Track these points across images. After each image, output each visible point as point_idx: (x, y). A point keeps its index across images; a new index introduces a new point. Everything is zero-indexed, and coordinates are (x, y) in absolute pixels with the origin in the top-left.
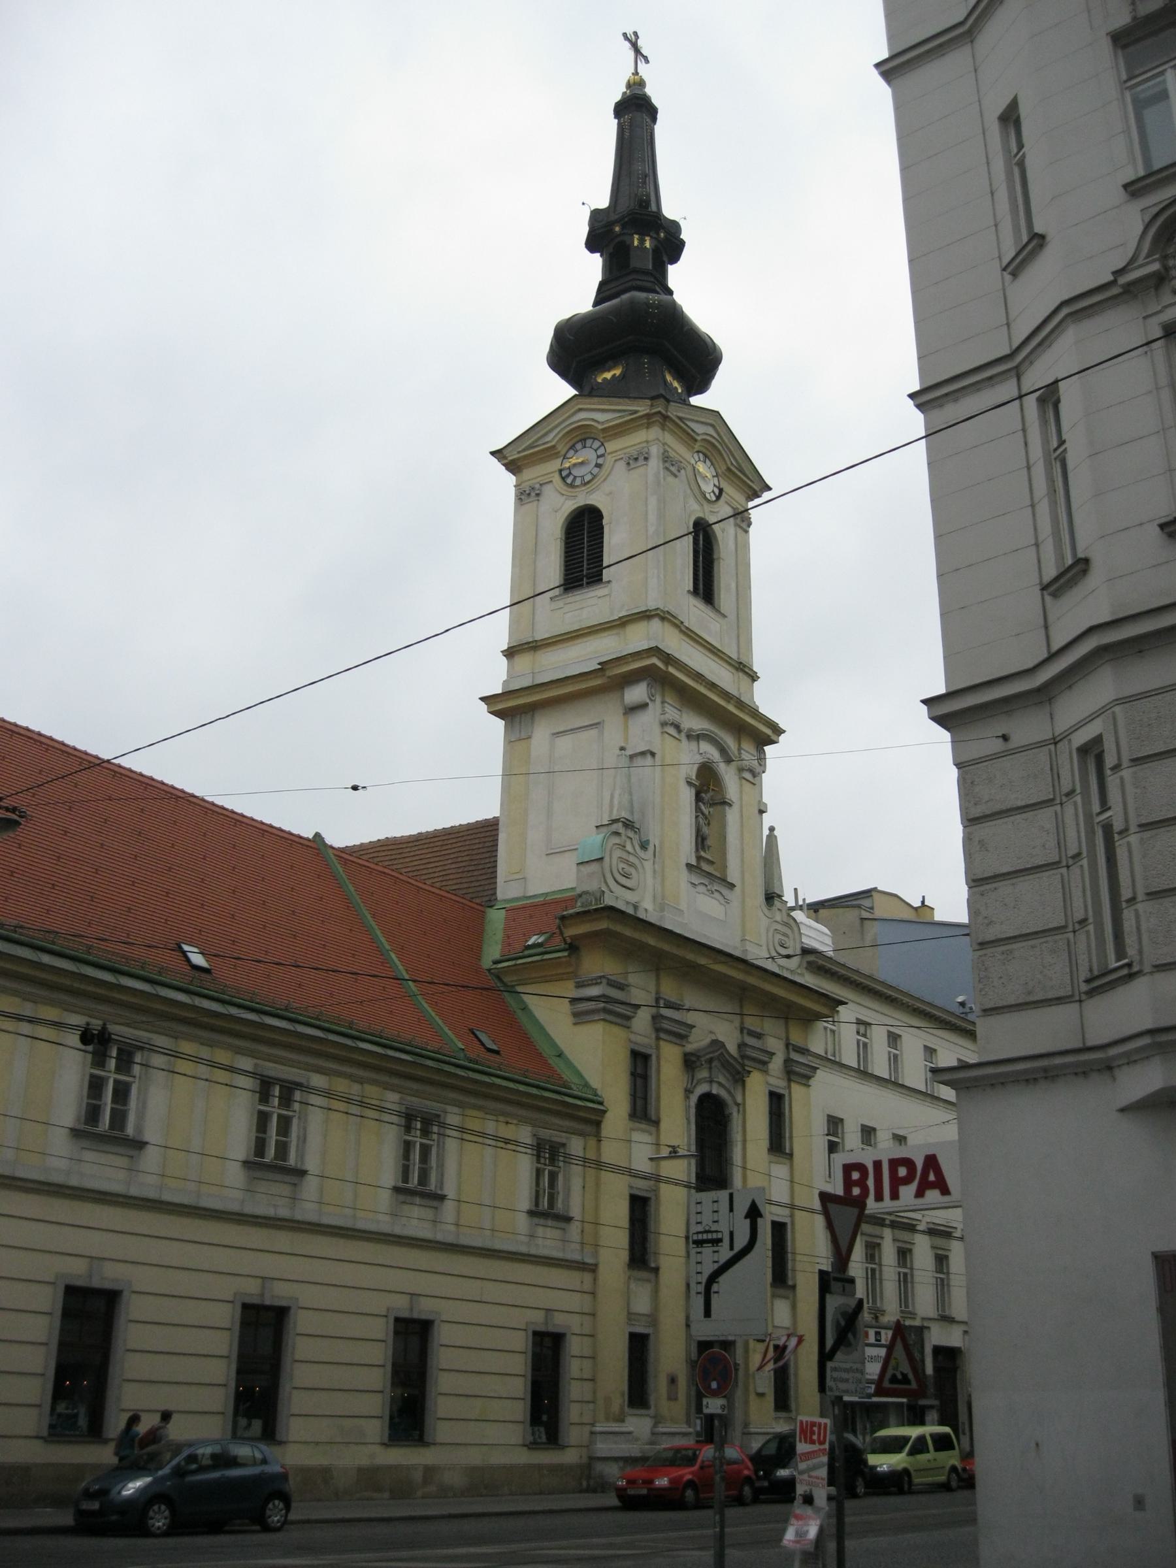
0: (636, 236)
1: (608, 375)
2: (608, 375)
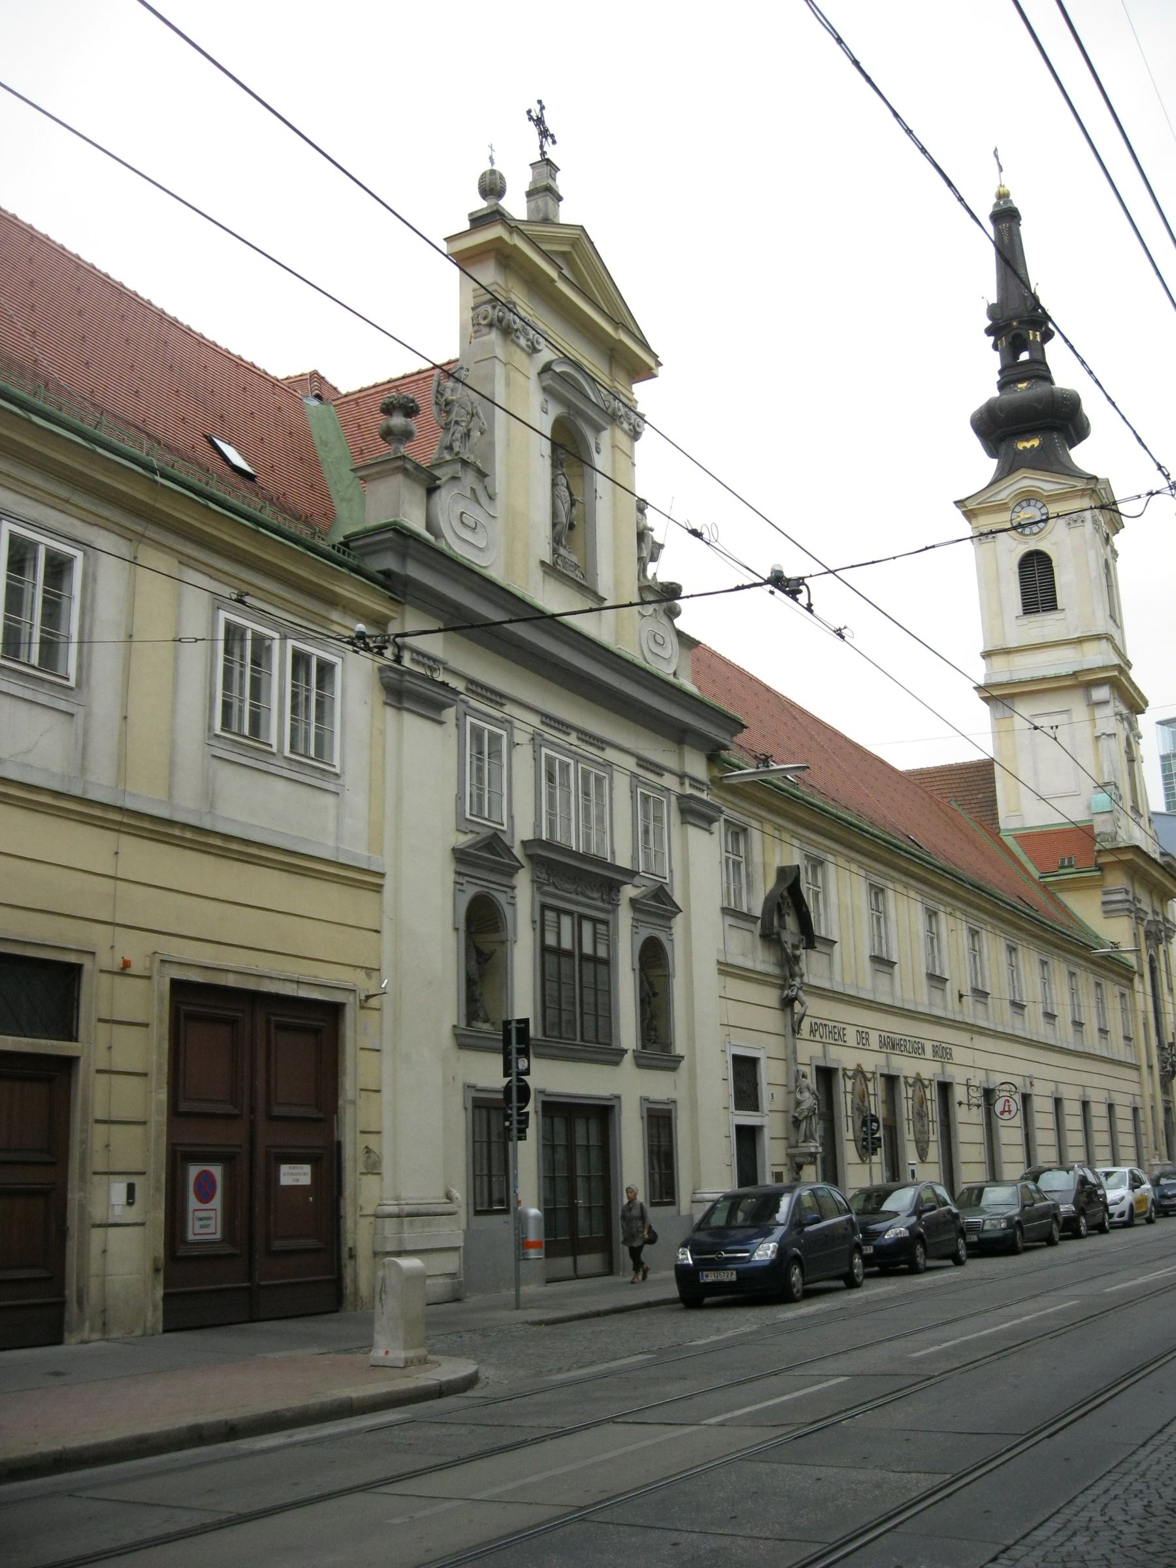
0: (1031, 332)
1: (1028, 445)
2: (1028, 445)
